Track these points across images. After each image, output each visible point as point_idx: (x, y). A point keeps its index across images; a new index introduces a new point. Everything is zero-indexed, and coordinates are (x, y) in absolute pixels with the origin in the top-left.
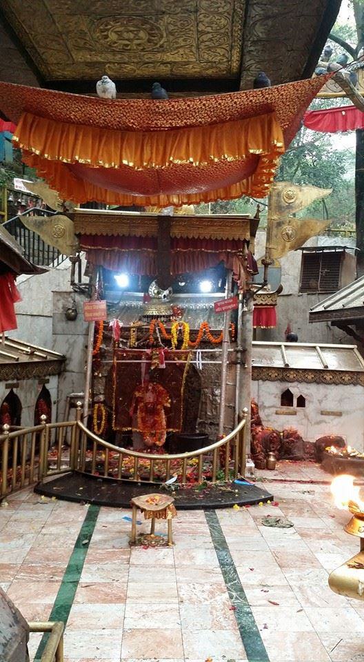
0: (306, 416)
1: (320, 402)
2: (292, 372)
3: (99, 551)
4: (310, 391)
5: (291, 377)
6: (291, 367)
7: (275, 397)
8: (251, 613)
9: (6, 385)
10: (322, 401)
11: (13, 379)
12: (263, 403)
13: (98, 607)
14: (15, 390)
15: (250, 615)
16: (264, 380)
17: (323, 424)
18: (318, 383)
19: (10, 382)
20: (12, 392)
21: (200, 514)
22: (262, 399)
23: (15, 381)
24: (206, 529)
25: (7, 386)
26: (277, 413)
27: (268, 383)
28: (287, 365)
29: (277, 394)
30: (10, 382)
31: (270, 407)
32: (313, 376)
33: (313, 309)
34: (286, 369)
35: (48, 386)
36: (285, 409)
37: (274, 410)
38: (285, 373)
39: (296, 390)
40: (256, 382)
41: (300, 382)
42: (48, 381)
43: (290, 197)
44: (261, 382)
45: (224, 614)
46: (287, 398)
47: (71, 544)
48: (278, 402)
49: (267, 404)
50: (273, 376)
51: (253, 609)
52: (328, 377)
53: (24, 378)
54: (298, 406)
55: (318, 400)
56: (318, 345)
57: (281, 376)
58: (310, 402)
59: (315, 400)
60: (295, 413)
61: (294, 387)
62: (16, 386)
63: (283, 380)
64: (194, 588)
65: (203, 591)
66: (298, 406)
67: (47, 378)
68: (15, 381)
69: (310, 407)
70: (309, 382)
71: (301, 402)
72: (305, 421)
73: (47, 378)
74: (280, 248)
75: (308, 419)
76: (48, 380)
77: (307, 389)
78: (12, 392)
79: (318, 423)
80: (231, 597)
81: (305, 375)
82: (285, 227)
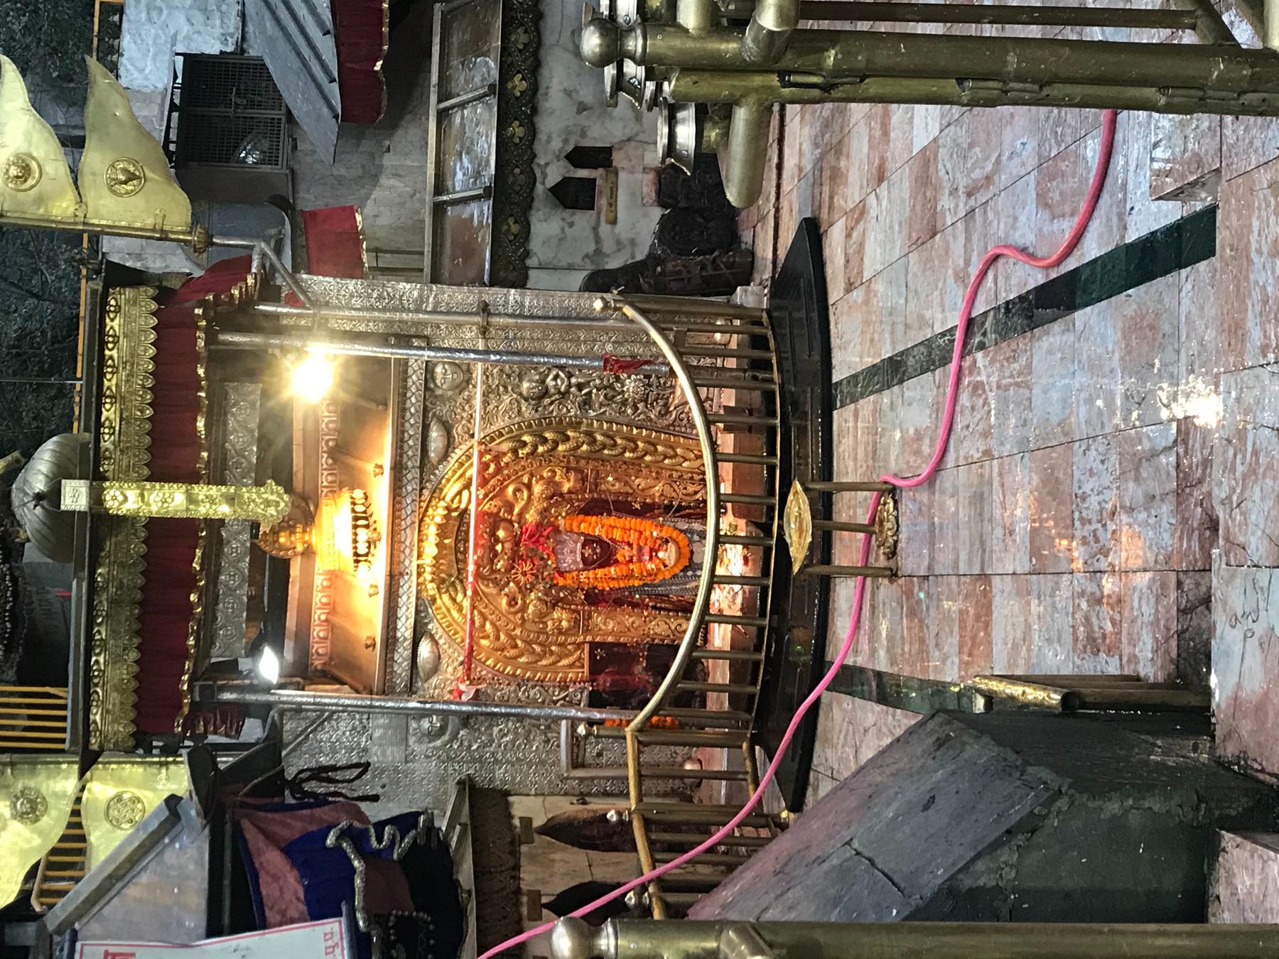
3: (906, 649)
4: (556, 126)
7: (571, 225)
8: (1007, 303)
9: (530, 919)
10: (581, 103)
12: (587, 256)
13: (997, 634)
14: (544, 900)
16: (527, 254)
18: (535, 111)
19: (524, 910)
21: (842, 418)
24: (867, 404)
27: (535, 245)
29: (563, 219)
31: (598, 240)
32: (516, 123)
35: (538, 822)
36: (602, 202)
40: (532, 273)
42: (527, 822)
44: (531, 262)
45: (1007, 360)
46: (574, 196)
47: (894, 717)
48: (583, 219)
49: (591, 248)
50: (515, 228)
51: (1001, 301)
53: (517, 879)
55: (579, 111)
58: (583, 134)
61: (545, 176)
64: (968, 427)
65: (973, 408)
67: (517, 822)
71: (579, 156)
73: (517, 822)
75: (629, 140)
76: (521, 819)
77: (548, 142)
80: (982, 346)
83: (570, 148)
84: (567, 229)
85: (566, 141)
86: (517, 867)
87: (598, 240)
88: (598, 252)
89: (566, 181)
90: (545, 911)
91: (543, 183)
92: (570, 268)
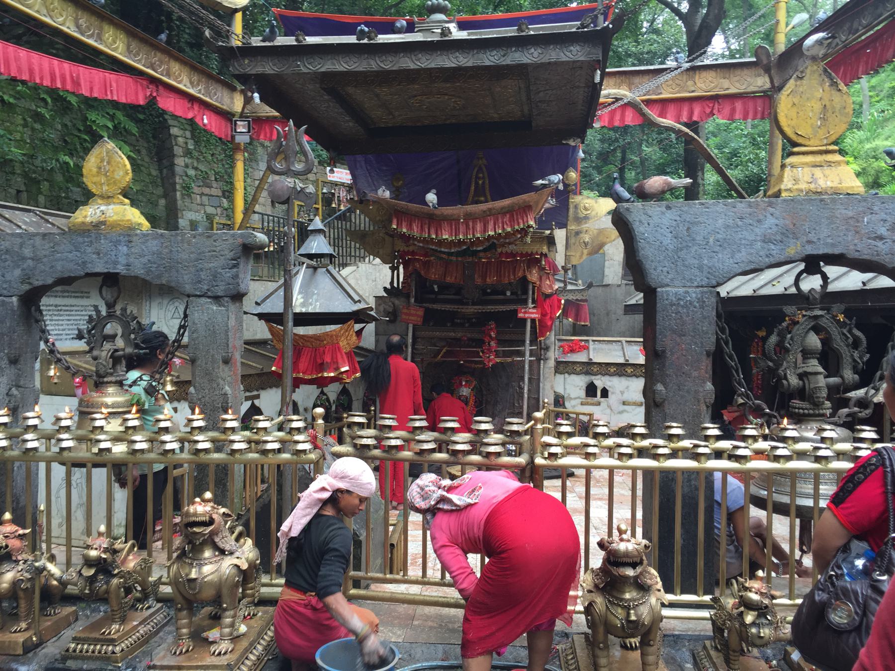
0: (609, 407)
1: (622, 393)
5: (595, 370)
6: (595, 360)
16: (569, 374)
17: (625, 414)
18: (620, 376)
22: (568, 391)
26: (582, 404)
27: (573, 377)
31: (575, 398)
34: (590, 363)
36: (590, 400)
37: (579, 401)
38: (589, 368)
39: (600, 382)
41: (604, 375)
43: (586, 209)
44: (566, 375)
46: (591, 390)
48: (583, 393)
49: (572, 396)
50: (578, 369)
52: (629, 370)
54: (602, 396)
56: (623, 339)
58: (613, 393)
59: (618, 392)
60: (599, 404)
63: (587, 373)
66: (602, 396)
69: (612, 398)
70: (611, 375)
71: (605, 393)
72: (608, 411)
74: (578, 254)
79: (621, 412)
81: (606, 369)
82: (582, 235)
87: (575, 398)
89: (595, 387)
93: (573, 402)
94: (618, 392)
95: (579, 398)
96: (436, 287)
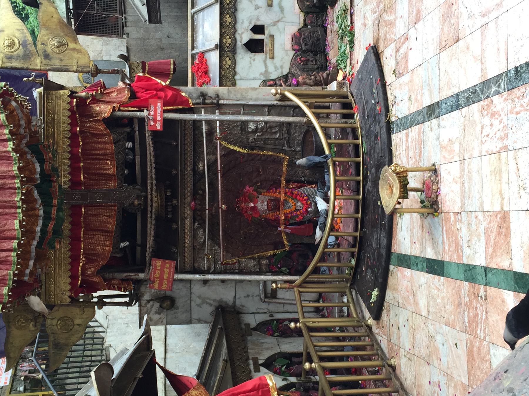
0: (275, 24)
1: (257, 7)
2: (224, 41)
3: (447, 248)
5: (229, 41)
6: (217, 41)
7: (254, 60)
8: (516, 68)
9: (255, 372)
10: (256, 5)
11: (248, 365)
12: (261, 74)
13: (515, 241)
14: (260, 362)
15: (519, 69)
16: (235, 73)
17: (284, 4)
18: (236, 10)
19: (252, 367)
20: (263, 365)
21: (395, 138)
22: (257, 76)
23: (251, 362)
24: (414, 131)
25: (257, 370)
26: (273, 58)
27: (238, 69)
28: (216, 45)
29: (251, 58)
30: (252, 367)
31: (266, 66)
32: (228, 16)
33: (144, 18)
34: (221, 47)
35: (253, 324)
36: (267, 48)
37: (269, 61)
38: (226, 49)
39: (244, 35)
40: (237, 82)
41: (235, 31)
42: (248, 325)
43: (12, 45)
44: (237, 77)
45: (518, 98)
46: (255, 46)
47: (439, 281)
48: (259, 57)
49: (263, 70)
50: (229, 62)
51: (512, 66)
53: (247, 352)
54: (263, 33)
55: (256, 9)
56: (190, 12)
57: (230, 54)
58: (258, 19)
59: (256, 13)
60: (272, 37)
61: (241, 38)
62: (256, 360)
63: (234, 51)
64: (488, 136)
65: (491, 125)
66: (263, 33)
67: (244, 327)
68: (251, 362)
69: (264, 20)
70: (235, 21)
71: (258, 29)
72: (280, 25)
73: (244, 327)
74: (76, 55)
75: (278, 21)
76: (245, 324)
77: (243, 23)
78: (263, 365)
79: (282, 9)
80: (498, 93)
81: (227, 28)
82: (49, 50)
83: (251, 26)
84: (252, 62)
85: (250, 23)
86: (246, 347)
87: (266, 66)
88: (266, 71)
90: (262, 368)
91: (241, 42)
92: (254, 79)
93: (271, 69)
94: (256, 13)
95: (265, 62)
96: (122, 245)
